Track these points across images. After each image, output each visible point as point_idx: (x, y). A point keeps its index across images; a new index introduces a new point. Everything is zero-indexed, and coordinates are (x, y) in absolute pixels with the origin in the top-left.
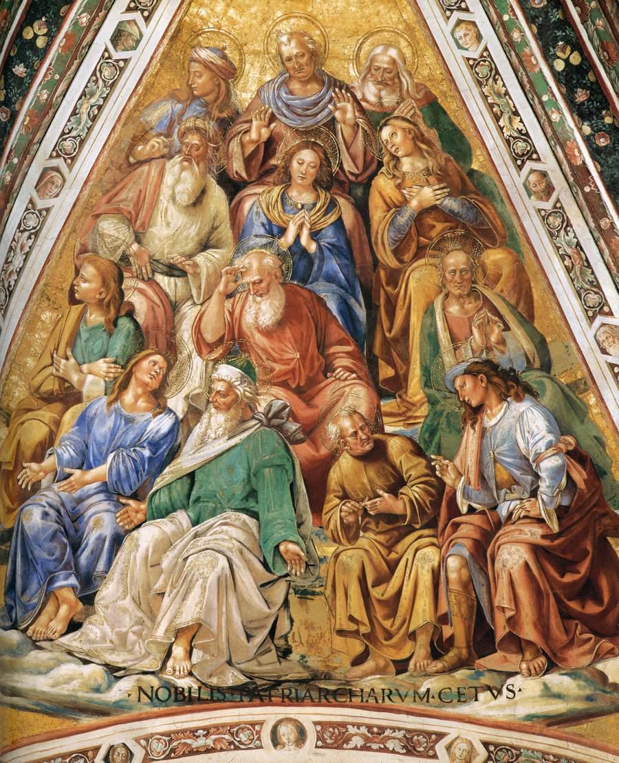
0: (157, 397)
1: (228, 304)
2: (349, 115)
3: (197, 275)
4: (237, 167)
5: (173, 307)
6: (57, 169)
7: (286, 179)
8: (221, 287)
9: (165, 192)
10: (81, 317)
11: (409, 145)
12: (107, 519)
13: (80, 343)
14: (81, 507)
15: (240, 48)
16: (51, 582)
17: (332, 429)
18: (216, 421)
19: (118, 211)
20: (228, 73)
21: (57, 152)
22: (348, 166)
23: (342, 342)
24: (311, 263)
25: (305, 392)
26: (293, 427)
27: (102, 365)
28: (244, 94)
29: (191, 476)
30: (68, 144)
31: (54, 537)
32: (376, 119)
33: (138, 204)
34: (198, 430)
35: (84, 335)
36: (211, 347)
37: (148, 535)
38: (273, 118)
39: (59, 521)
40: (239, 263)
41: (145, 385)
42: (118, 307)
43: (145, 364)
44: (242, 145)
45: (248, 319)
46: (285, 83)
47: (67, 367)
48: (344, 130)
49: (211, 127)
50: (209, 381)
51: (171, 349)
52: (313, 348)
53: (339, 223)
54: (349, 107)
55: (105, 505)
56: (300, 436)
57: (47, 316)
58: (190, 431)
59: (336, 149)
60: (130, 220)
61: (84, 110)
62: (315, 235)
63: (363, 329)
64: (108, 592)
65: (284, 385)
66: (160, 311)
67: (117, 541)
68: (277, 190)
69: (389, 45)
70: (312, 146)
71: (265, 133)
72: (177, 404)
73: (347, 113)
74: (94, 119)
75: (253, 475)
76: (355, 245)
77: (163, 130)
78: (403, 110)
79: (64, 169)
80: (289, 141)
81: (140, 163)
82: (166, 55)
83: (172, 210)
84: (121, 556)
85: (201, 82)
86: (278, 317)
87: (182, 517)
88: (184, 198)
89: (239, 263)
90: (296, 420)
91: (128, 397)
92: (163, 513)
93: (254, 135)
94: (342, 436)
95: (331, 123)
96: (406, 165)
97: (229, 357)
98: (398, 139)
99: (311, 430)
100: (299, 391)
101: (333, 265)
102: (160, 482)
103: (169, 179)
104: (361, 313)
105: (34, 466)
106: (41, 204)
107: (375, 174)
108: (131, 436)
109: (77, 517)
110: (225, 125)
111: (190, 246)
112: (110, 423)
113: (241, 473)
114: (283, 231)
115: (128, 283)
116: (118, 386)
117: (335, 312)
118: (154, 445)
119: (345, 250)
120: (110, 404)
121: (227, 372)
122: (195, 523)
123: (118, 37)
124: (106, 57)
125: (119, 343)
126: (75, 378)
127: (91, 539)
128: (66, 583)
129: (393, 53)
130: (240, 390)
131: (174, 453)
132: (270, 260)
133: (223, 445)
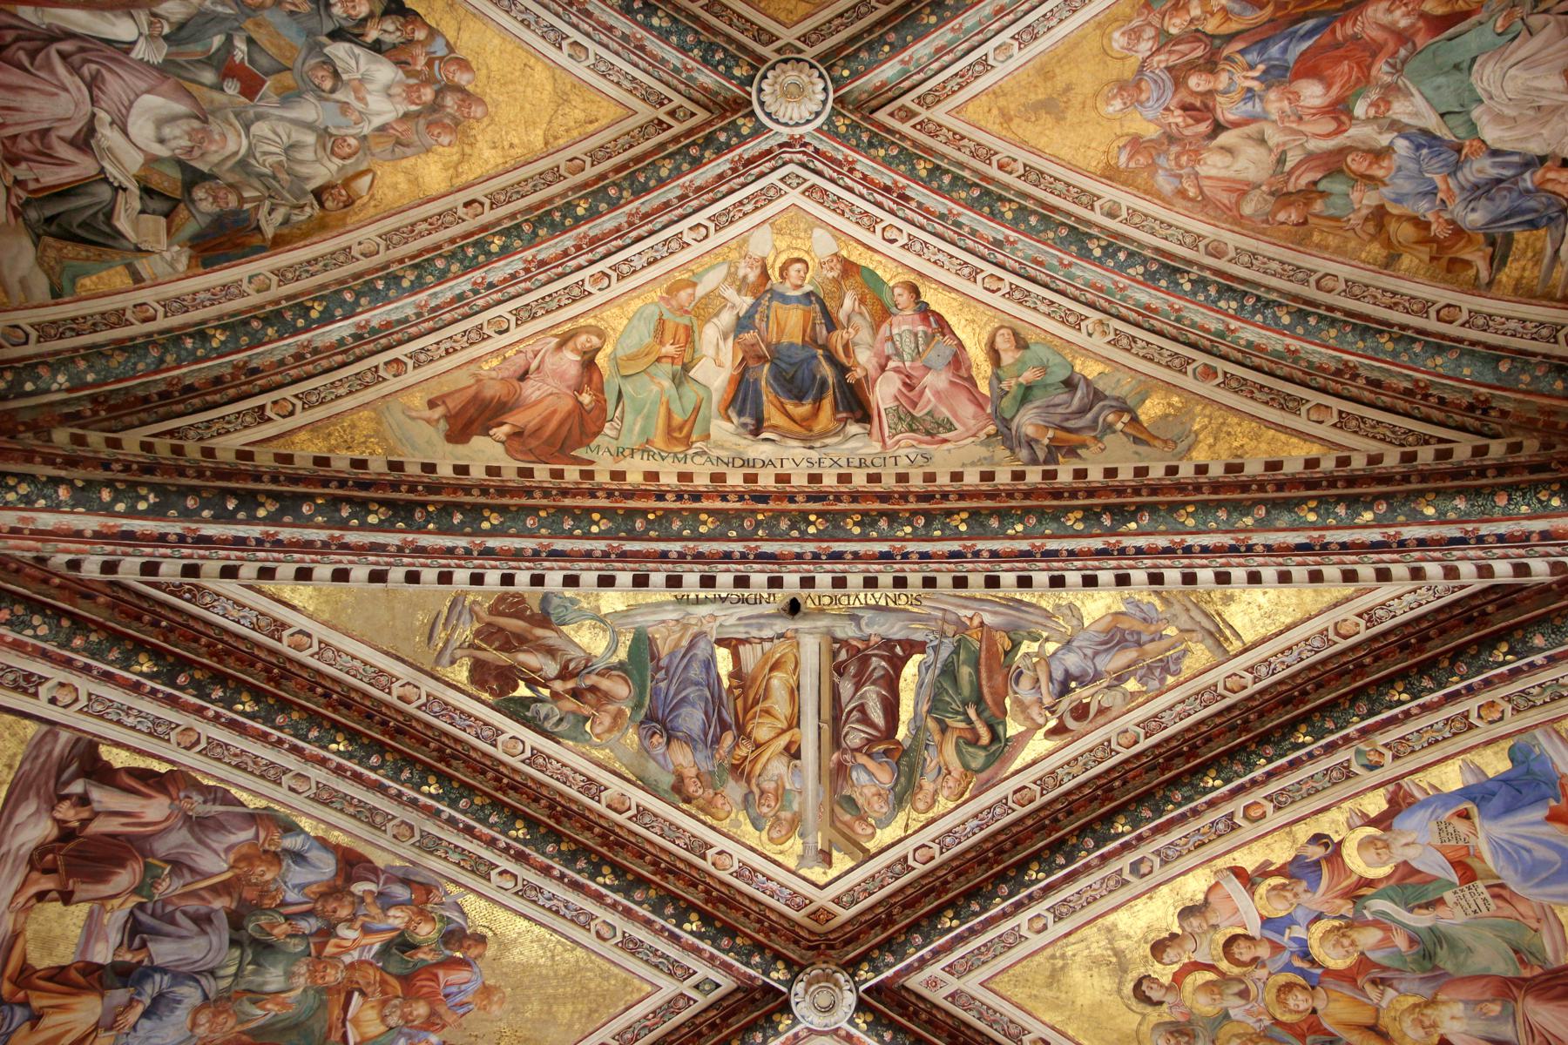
0: (1379, 154)
1: (1306, 118)
2: (1162, 57)
3: (1284, 144)
4: (1203, 128)
5: (1310, 157)
6: (1206, 246)
7: (1211, 93)
8: (1294, 126)
9: (1223, 173)
10: (1316, 216)
11: (1182, 13)
12: (1476, 166)
13: (1337, 213)
14: (1467, 185)
15: (1118, 137)
16: (1528, 191)
17: (1403, 23)
18: (1400, 110)
19: (1238, 204)
20: (1136, 144)
21: (1195, 247)
22: (1199, 52)
23: (1333, 32)
24: (1274, 66)
25: (1375, 50)
26: (1403, 52)
27: (1355, 196)
28: (1152, 132)
29: (1442, 115)
30: (1188, 240)
31: (1491, 199)
32: (1165, 41)
33: (1230, 190)
34: (1405, 119)
35: (1332, 211)
36: (1340, 123)
37: (1492, 134)
38: (1167, 109)
39: (1478, 198)
40: (1275, 116)
41: (1370, 164)
42: (1311, 193)
43: (1354, 167)
44: (1188, 126)
45: (1318, 102)
46: (1141, 103)
47: (1355, 220)
48: (1173, 60)
49: (1175, 149)
50: (1368, 120)
51: (1343, 152)
52: (1341, 52)
53: (1242, 52)
54: (1156, 59)
55: (1466, 170)
56: (1410, 45)
57: (1316, 238)
58: (1407, 125)
59: (1189, 62)
60: (1243, 194)
61: (1164, 232)
62: (1252, 67)
63: (1322, 19)
64: (1535, 148)
65: (1369, 68)
66: (1313, 164)
67: (1495, 153)
68: (1219, 99)
69: (1110, 39)
70: (1186, 78)
71: (1178, 112)
72: (1384, 140)
73: (1161, 60)
74: (1170, 226)
75: (1440, 71)
76: (1257, 38)
77: (1176, 181)
78: (1156, 22)
79: (1206, 241)
80: (1182, 95)
81: (1202, 192)
82: (1124, 183)
83: (1237, 167)
84: (1506, 147)
85: (1142, 160)
86: (1316, 82)
87: (1476, 113)
88: (1228, 159)
89: (1275, 116)
90: (1397, 52)
91: (1380, 173)
92: (1473, 126)
93: (1180, 120)
94: (1408, 14)
95: (1169, 69)
96: (1196, 11)
97: (1349, 112)
98: (1177, 21)
99: (1402, 37)
100: (1374, 55)
101: (1274, 51)
102: (1448, 136)
103: (1213, 172)
104: (1310, 24)
105: (1433, 227)
106: (1232, 254)
107: (1204, 33)
108: (1412, 166)
109: (1476, 187)
110: (1171, 139)
111: (1262, 151)
112: (1399, 181)
113: (1441, 80)
114: (1249, 90)
115: (1291, 188)
116: (1372, 181)
117: (1310, 42)
118: (1419, 147)
119: (1263, 43)
120: (1385, 185)
121: (1360, 109)
122: (1481, 101)
123: (1112, 215)
124: (1126, 222)
125: (1336, 186)
126: (1364, 212)
127: (1494, 172)
128: (1528, 181)
129: (1116, 35)
130: (1374, 95)
131: (1425, 132)
132: (1272, 95)
133: (1418, 99)
